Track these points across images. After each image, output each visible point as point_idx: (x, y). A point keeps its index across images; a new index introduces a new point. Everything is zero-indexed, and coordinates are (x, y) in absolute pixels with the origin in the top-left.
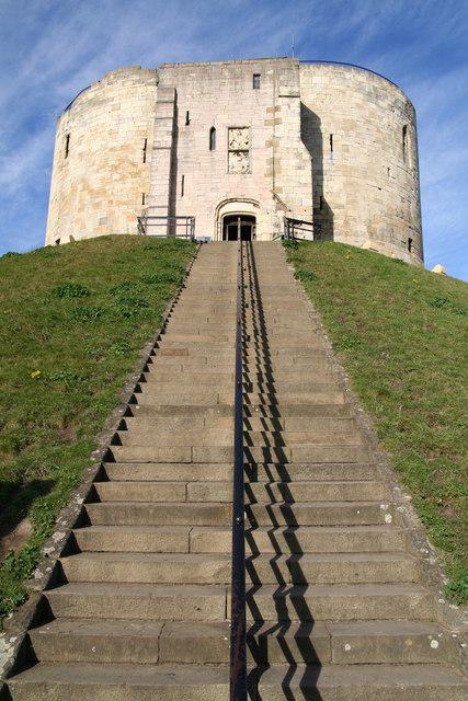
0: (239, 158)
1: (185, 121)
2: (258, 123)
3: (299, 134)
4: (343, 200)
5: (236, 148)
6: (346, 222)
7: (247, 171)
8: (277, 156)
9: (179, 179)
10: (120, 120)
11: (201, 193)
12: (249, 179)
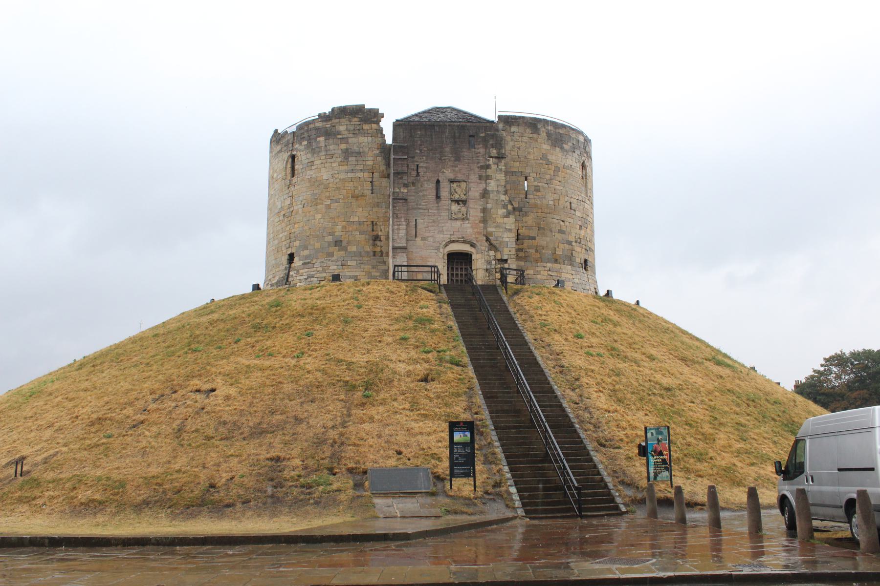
1: (414, 173)
6: (537, 251)
8: (489, 206)
10: (347, 154)
11: (431, 234)
12: (467, 225)
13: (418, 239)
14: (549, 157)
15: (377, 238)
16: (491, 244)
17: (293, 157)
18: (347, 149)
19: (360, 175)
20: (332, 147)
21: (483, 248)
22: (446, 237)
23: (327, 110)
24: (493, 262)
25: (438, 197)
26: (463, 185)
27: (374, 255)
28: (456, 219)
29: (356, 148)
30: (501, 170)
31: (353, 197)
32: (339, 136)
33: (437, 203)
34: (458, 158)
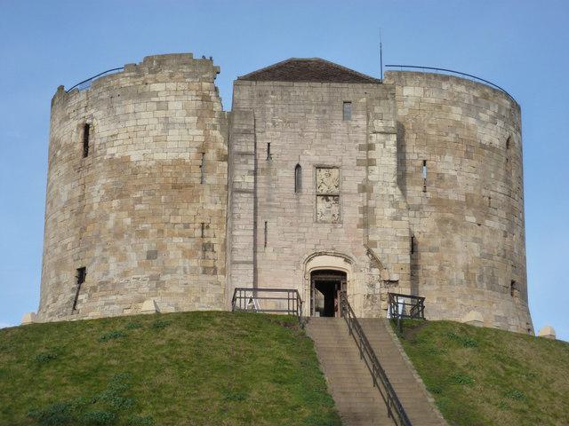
0: (328, 204)
1: (266, 155)
3: (395, 179)
4: (438, 241)
5: (324, 192)
6: (441, 269)
7: (337, 222)
8: (372, 203)
9: (261, 226)
10: (167, 124)
11: (287, 243)
13: (269, 249)
14: (459, 131)
15: (207, 247)
16: (374, 258)
17: (87, 127)
21: (363, 264)
22: (310, 248)
23: (138, 60)
24: (378, 285)
25: (298, 187)
26: (335, 173)
27: (204, 273)
28: (325, 222)
30: (389, 151)
31: (174, 187)
32: (157, 99)
33: (297, 199)
34: (327, 135)
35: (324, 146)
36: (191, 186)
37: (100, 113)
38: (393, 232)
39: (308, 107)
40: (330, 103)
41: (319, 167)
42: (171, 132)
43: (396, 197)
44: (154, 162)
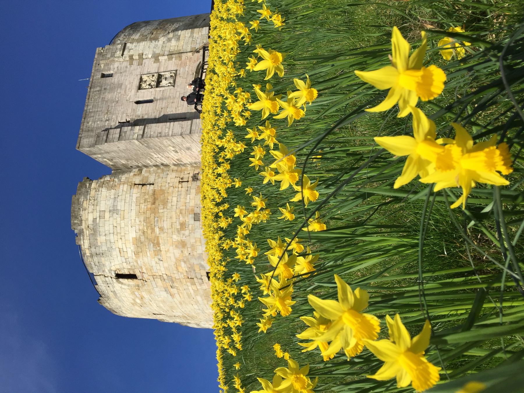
2: (139, 70)
10: (114, 211)
12: (181, 71)
17: (119, 276)
18: (110, 211)
19: (135, 196)
20: (107, 228)
29: (110, 203)
30: (136, 46)
31: (154, 203)
32: (98, 219)
34: (120, 86)
35: (126, 87)
36: (154, 192)
37: (107, 263)
38: (187, 38)
39: (100, 100)
40: (101, 87)
41: (140, 88)
42: (119, 208)
43: (165, 40)
44: (137, 219)
